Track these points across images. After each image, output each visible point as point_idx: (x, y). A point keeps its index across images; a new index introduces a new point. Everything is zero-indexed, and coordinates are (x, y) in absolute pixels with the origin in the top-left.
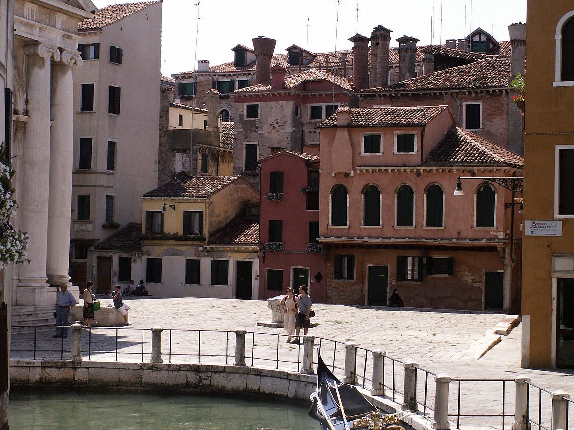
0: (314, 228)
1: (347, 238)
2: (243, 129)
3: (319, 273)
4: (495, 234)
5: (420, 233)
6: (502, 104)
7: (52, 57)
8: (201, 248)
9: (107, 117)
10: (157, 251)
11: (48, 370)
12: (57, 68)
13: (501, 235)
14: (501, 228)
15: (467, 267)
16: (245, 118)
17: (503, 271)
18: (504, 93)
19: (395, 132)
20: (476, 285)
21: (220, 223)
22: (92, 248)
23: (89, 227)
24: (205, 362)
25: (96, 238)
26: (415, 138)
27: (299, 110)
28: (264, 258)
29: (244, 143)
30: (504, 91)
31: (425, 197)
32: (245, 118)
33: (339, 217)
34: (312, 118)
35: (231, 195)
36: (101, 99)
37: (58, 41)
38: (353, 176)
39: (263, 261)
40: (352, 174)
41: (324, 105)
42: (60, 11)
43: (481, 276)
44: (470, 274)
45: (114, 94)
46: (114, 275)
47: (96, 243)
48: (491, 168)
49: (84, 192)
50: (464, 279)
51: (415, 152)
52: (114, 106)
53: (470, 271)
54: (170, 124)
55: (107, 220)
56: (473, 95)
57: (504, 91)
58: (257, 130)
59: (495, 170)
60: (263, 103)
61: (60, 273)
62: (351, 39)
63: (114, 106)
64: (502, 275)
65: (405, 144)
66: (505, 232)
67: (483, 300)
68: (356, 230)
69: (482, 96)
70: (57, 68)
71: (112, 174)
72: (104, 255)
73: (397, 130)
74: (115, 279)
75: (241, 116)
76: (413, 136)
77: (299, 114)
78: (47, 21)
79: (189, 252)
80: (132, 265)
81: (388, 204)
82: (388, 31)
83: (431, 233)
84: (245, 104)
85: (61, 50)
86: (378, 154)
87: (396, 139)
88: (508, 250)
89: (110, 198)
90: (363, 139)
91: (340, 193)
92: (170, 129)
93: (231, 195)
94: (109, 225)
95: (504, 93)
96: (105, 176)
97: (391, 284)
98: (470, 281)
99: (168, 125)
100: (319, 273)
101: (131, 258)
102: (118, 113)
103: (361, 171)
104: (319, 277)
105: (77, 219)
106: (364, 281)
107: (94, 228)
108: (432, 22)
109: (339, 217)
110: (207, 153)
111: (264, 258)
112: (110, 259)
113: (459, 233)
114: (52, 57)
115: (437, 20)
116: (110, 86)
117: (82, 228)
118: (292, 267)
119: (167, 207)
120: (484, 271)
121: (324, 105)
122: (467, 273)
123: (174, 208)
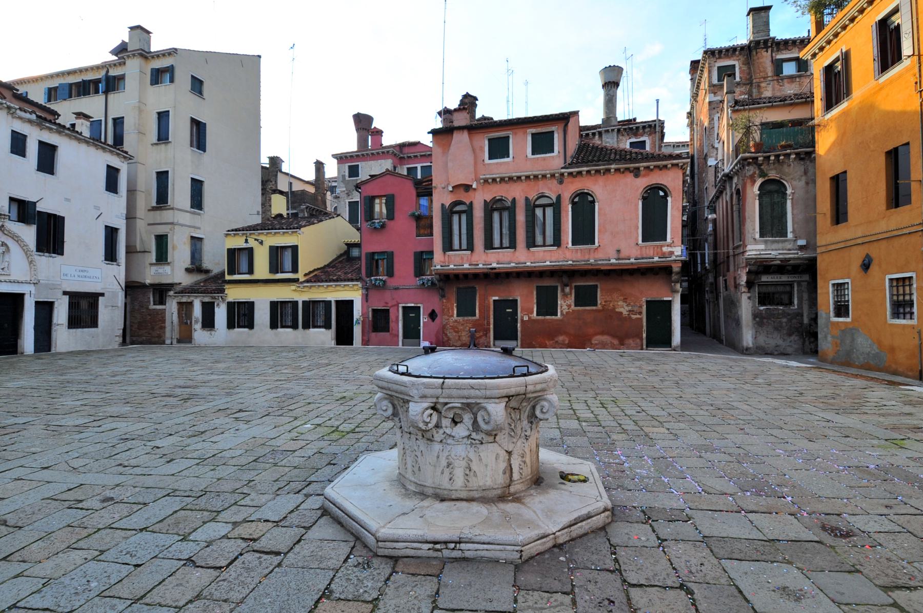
3: (433, 311)
4: (670, 249)
5: (568, 255)
14: (678, 240)
16: (347, 178)
18: (597, 137)
20: (634, 317)
22: (171, 293)
23: (167, 269)
25: (176, 281)
26: (556, 135)
28: (367, 295)
29: (347, 201)
31: (570, 209)
32: (347, 178)
36: (180, 130)
39: (366, 298)
40: (474, 186)
41: (419, 166)
43: (641, 307)
44: (625, 304)
46: (196, 322)
47: (178, 288)
48: (664, 163)
49: (161, 230)
50: (617, 310)
53: (625, 300)
55: (192, 263)
65: (542, 144)
67: (644, 335)
71: (199, 214)
72: (184, 300)
74: (198, 326)
75: (344, 176)
76: (553, 132)
80: (216, 309)
83: (579, 254)
86: (506, 160)
87: (529, 138)
89: (196, 241)
90: (487, 142)
94: (196, 267)
95: (597, 137)
98: (625, 313)
100: (433, 311)
101: (213, 303)
102: (204, 151)
103: (486, 181)
104: (433, 315)
105: (154, 261)
107: (172, 270)
108: (508, 101)
111: (367, 295)
112: (191, 304)
113: (619, 251)
115: (510, 100)
117: (161, 271)
118: (401, 305)
120: (644, 299)
121: (419, 166)
122: (620, 303)
123: (261, 243)
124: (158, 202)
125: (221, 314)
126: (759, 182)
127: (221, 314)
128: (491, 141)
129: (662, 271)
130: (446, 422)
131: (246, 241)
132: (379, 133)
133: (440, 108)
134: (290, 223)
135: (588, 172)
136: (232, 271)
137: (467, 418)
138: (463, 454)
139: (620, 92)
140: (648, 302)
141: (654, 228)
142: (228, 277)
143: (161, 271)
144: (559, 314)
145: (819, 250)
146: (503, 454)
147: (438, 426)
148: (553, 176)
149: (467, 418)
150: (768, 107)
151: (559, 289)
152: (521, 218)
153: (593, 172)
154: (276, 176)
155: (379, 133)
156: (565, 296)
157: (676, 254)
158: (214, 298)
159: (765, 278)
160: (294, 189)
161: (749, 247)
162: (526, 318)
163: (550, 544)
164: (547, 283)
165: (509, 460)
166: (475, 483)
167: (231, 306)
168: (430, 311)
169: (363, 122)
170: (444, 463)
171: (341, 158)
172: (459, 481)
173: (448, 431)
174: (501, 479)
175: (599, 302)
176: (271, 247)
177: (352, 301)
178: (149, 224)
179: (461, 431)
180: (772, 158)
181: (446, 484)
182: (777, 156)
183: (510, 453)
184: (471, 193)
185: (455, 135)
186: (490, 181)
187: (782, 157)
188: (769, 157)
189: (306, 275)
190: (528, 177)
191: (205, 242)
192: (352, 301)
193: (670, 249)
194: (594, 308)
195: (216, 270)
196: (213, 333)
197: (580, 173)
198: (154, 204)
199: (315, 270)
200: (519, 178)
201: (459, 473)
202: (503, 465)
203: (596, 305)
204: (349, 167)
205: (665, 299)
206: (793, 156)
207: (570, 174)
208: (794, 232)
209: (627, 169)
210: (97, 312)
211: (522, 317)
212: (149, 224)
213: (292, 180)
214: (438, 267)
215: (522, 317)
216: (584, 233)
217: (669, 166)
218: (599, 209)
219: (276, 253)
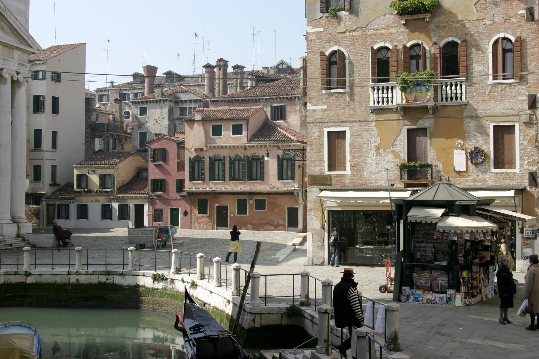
3: (186, 211)
7: (12, 78)
8: (112, 197)
10: (84, 200)
11: (9, 277)
12: (15, 84)
18: (297, 99)
21: (124, 181)
22: (43, 199)
24: (109, 269)
26: (243, 127)
29: (139, 131)
35: (130, 163)
37: (16, 67)
42: (17, 48)
45: (55, 101)
49: (37, 163)
52: (55, 110)
55: (52, 181)
56: (279, 100)
61: (19, 215)
62: (203, 67)
63: (55, 110)
64: (297, 208)
70: (15, 84)
71: (55, 152)
72: (51, 203)
76: (242, 125)
78: (8, 55)
79: (103, 200)
82: (227, 62)
85: (18, 73)
87: (231, 127)
88: (300, 194)
89: (54, 167)
90: (211, 127)
93: (130, 163)
94: (54, 183)
95: (297, 99)
96: (51, 153)
100: (186, 211)
102: (58, 113)
103: (211, 147)
104: (186, 213)
106: (214, 215)
114: (12, 78)
117: (37, 186)
119: (90, 172)
120: (286, 207)
124: (35, 147)
128: (213, 127)
135: (257, 146)
140: (289, 209)
143: (37, 186)
148: (242, 146)
152: (227, 166)
162: (232, 215)
168: (184, 211)
176: (100, 175)
178: (30, 159)
184: (203, 152)
190: (230, 147)
194: (264, 211)
197: (253, 146)
198: (33, 148)
200: (226, 147)
207: (249, 146)
212: (30, 159)
219: (103, 178)
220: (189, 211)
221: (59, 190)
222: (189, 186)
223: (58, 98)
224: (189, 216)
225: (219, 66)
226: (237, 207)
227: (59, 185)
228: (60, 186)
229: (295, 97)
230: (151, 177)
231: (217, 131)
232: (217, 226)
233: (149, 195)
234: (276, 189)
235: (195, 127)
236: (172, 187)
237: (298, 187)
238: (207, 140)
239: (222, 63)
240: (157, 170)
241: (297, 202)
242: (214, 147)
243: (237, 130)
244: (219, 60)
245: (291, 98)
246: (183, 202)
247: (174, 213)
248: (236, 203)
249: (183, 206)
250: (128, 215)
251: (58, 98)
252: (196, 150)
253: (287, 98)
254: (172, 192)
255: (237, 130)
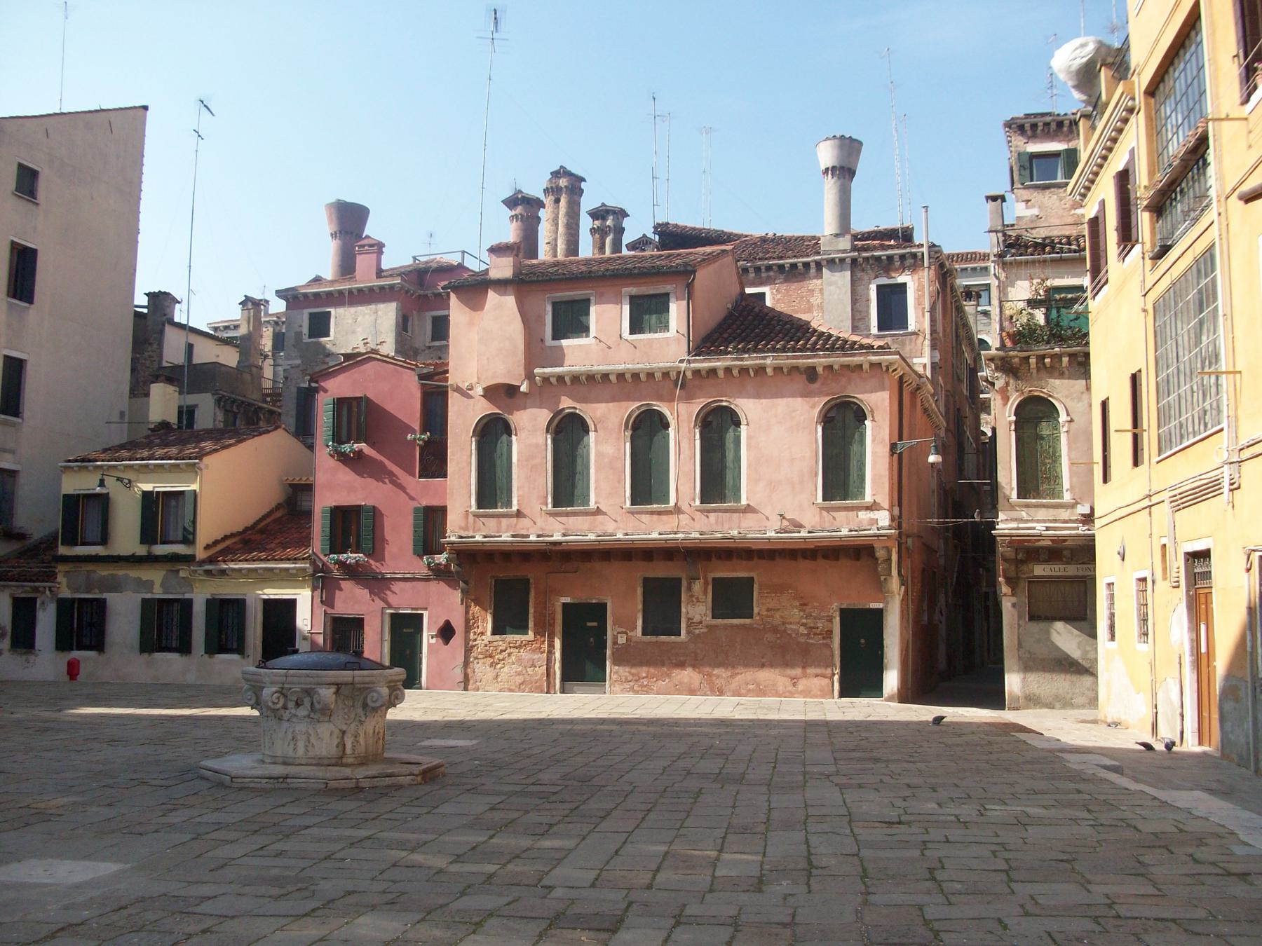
0: (432, 518)
1: (513, 536)
2: (301, 357)
6: (812, 291)
9: (4, 306)
13: (883, 518)
15: (795, 598)
16: (306, 339)
17: (880, 606)
18: (813, 271)
19: (625, 290)
27: (410, 323)
30: (813, 265)
32: (306, 339)
33: (492, 490)
34: (433, 339)
38: (525, 394)
40: (523, 388)
43: (830, 620)
51: (672, 332)
54: (165, 358)
56: (752, 275)
57: (813, 265)
58: (327, 360)
59: (866, 366)
60: (341, 310)
64: (879, 614)
66: (891, 510)
68: (532, 518)
69: (769, 277)
71: (13, 425)
73: (629, 285)
75: (299, 334)
77: (410, 329)
81: (607, 452)
84: (306, 312)
90: (549, 308)
91: (492, 433)
92: (165, 364)
95: (813, 271)
97: (615, 643)
99: (161, 356)
101: (35, 599)
103: (546, 379)
104: (446, 632)
109: (492, 490)
110: (235, 410)
116: (13, 243)
120: (835, 606)
125: (46, 622)
126: (1015, 399)
127: (46, 622)
129: (858, 554)
130: (291, 705)
131: (102, 483)
132: (379, 247)
133: (508, 193)
134: (181, 436)
135: (728, 370)
136: (71, 540)
137: (307, 701)
138: (304, 730)
139: (856, 184)
140: (843, 612)
141: (839, 478)
142: (63, 550)
144: (683, 632)
145: (1098, 523)
146: (337, 732)
147: (285, 707)
149: (307, 701)
150: (1053, 260)
151: (684, 583)
153: (735, 372)
154: (162, 332)
155: (379, 247)
156: (694, 600)
157: (881, 524)
158: (36, 590)
159: (1040, 570)
160: (195, 362)
161: (1002, 516)
163: (353, 785)
164: (661, 570)
165: (343, 737)
166: (311, 754)
167: (65, 607)
168: (441, 623)
169: (350, 220)
170: (290, 737)
171: (292, 297)
172: (301, 751)
173: (293, 711)
174: (334, 751)
175: (756, 610)
177: (295, 601)
179: (302, 712)
180: (1033, 361)
181: (291, 754)
182: (1041, 358)
183: (344, 732)
185: (491, 295)
186: (553, 380)
187: (1047, 360)
188: (1028, 358)
189: (207, 547)
191: (22, 480)
192: (295, 601)
193: (871, 515)
194: (747, 621)
195: (37, 532)
196: (32, 658)
199: (226, 538)
200: (606, 376)
201: (301, 745)
202: (336, 741)
203: (751, 617)
204: (311, 314)
205: (873, 606)
206: (1065, 360)
208: (1072, 489)
209: (795, 369)
210: (14, 612)
211: (615, 638)
213: (193, 339)
214: (453, 539)
215: (615, 638)
216: (717, 482)
217: (866, 366)
218: (749, 438)
220: (458, 624)
221: (21, 554)
222: (465, 522)
223: (34, 252)
224: (457, 640)
225: (553, 191)
226: (640, 606)
227: (22, 537)
228: (28, 543)
229: (806, 265)
230: (323, 501)
231: (571, 320)
232: (564, 678)
233: (313, 563)
234: (804, 534)
235: (488, 305)
236: (399, 536)
237: (890, 527)
238: (535, 352)
239: (563, 182)
240: (346, 475)
241: (880, 587)
242: (561, 378)
243: (646, 313)
244: (556, 174)
245: (794, 266)
246: (439, 589)
247: (405, 630)
248: (640, 591)
249: (440, 604)
250: (241, 638)
251: (34, 252)
252: (492, 393)
253: (781, 267)
254: (399, 553)
255: (646, 313)
